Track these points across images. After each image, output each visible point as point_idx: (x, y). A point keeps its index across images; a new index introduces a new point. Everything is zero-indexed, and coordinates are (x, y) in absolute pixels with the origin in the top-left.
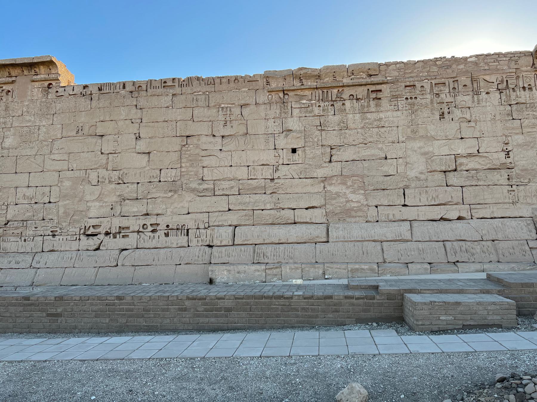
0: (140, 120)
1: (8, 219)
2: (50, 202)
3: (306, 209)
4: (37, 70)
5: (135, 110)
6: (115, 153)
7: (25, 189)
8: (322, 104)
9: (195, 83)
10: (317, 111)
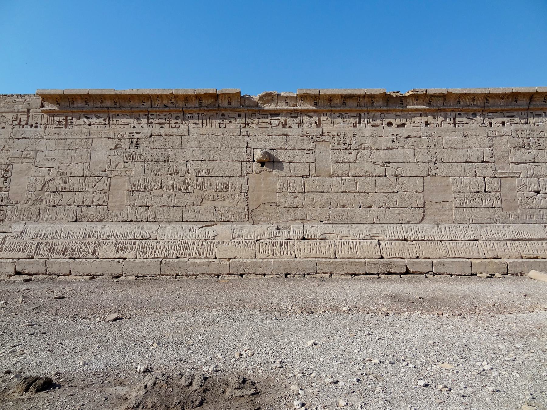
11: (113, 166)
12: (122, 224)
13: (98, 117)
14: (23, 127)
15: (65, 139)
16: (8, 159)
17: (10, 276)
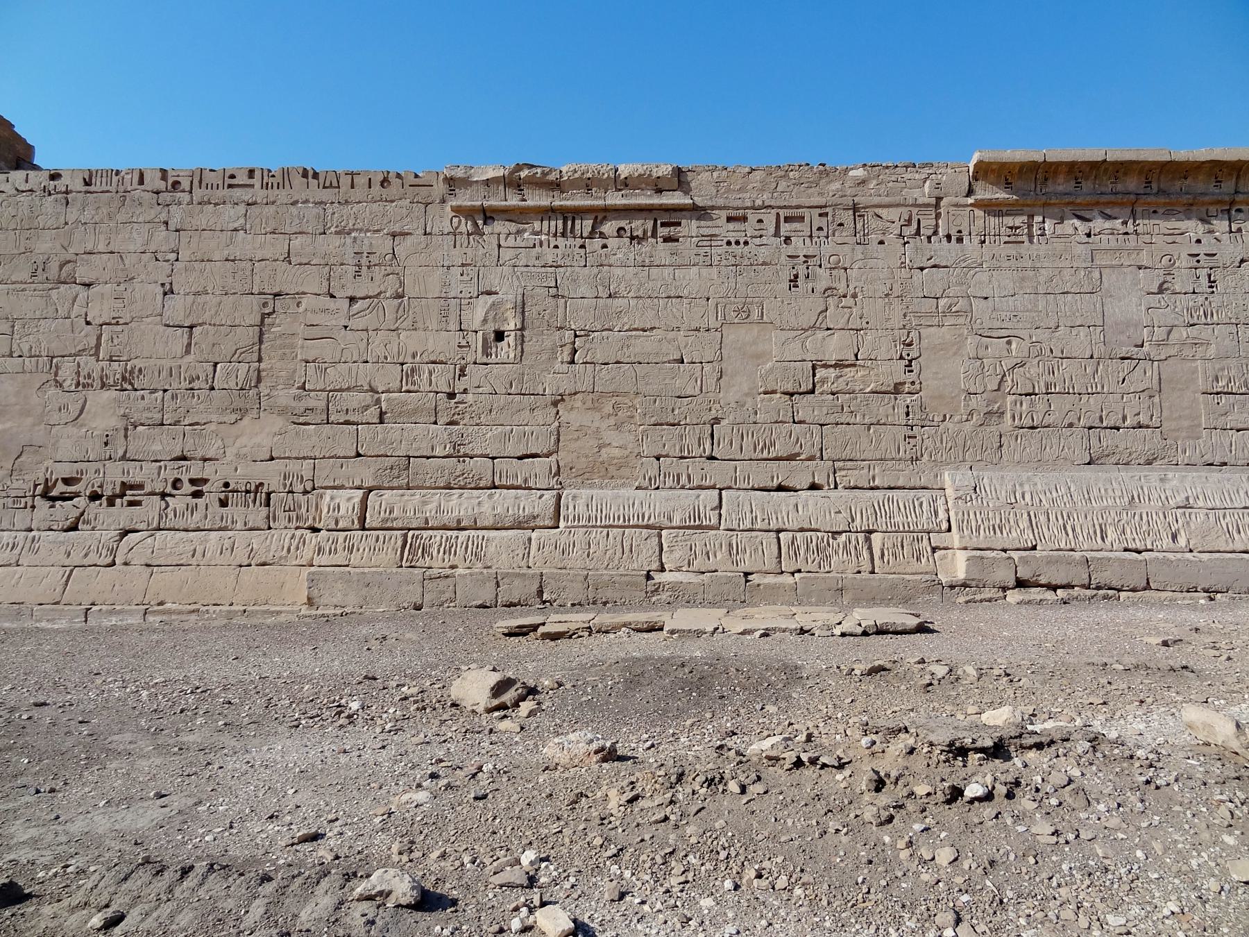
0: (173, 256)
3: (520, 458)
5: (164, 233)
6: (117, 323)
8: (561, 241)
9: (298, 180)
10: (549, 256)
11: (1160, 333)
12: (1205, 472)
13: (1109, 217)
14: (929, 238)
15: (1034, 269)
16: (905, 316)
17: (1004, 589)
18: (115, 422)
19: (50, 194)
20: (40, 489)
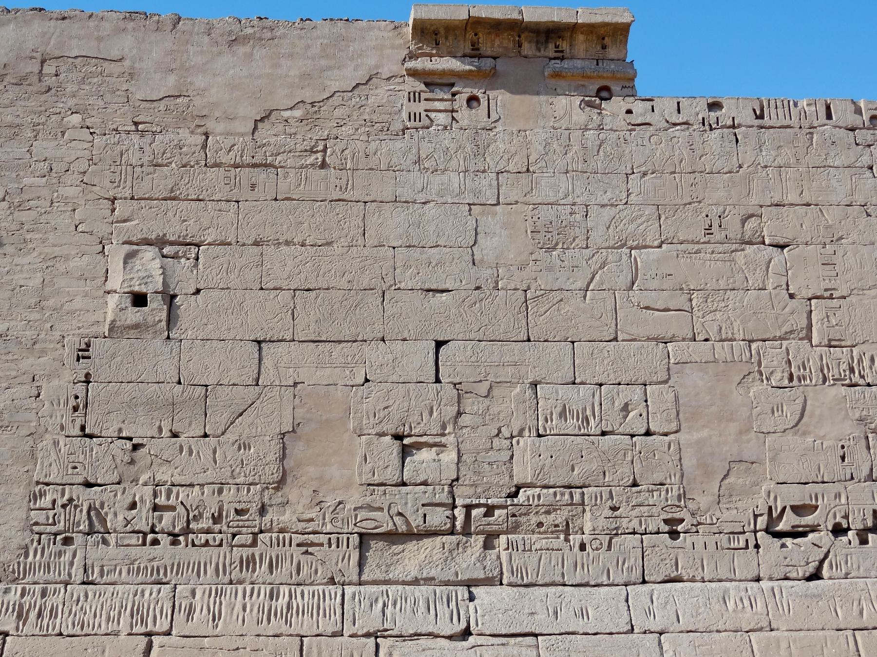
1: (515, 481)
2: (648, 433)
4: (564, 45)
6: (831, 297)
7: (565, 392)
18: (849, 430)
19: (711, 129)
20: (762, 522)
